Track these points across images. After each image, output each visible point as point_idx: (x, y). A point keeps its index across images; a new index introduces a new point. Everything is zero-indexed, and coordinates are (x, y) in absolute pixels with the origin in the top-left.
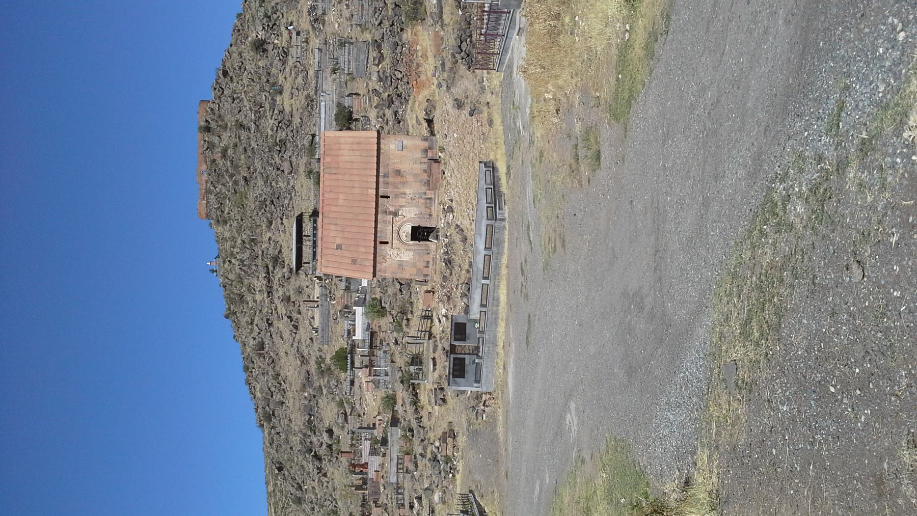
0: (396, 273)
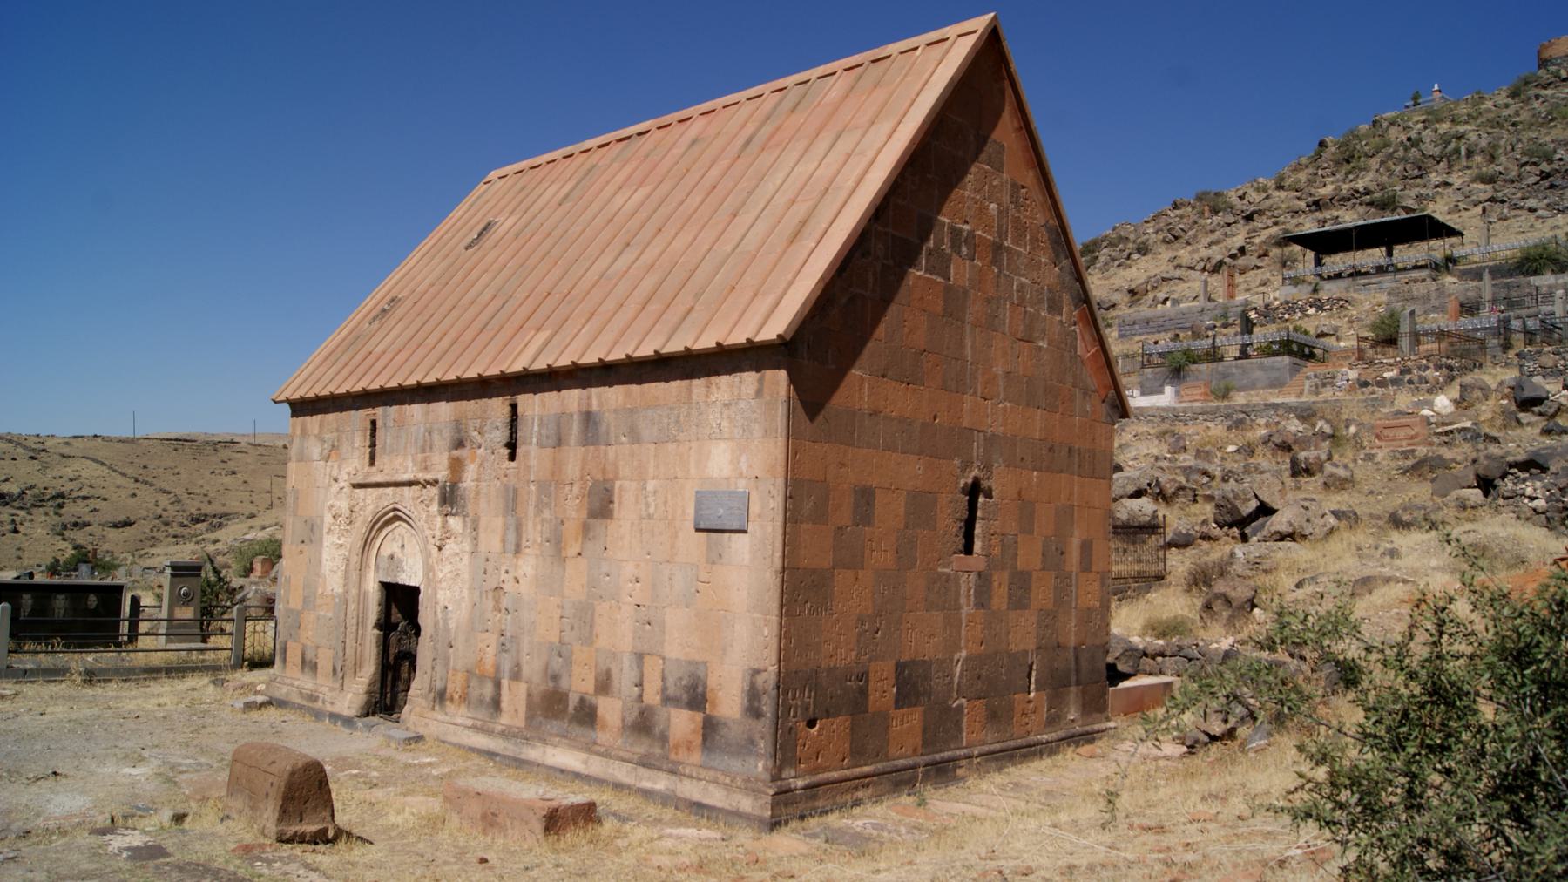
0: (295, 515)
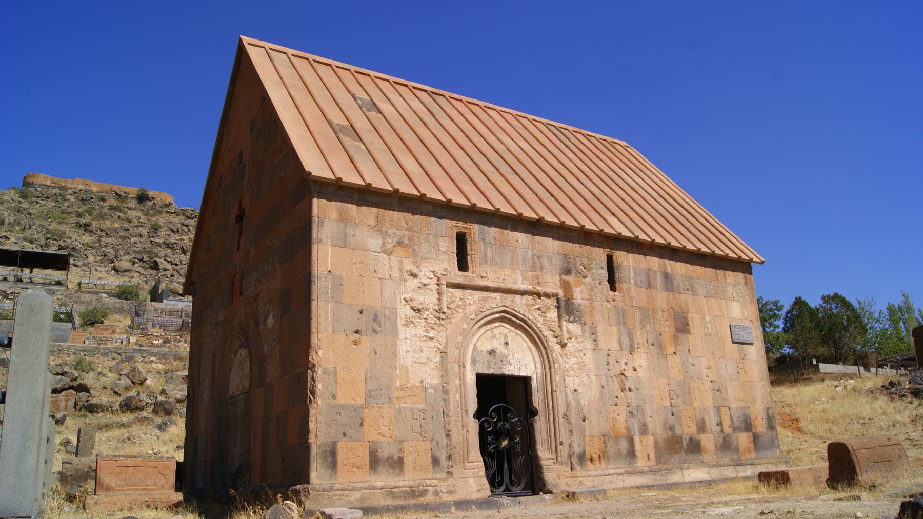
0: (338, 302)
